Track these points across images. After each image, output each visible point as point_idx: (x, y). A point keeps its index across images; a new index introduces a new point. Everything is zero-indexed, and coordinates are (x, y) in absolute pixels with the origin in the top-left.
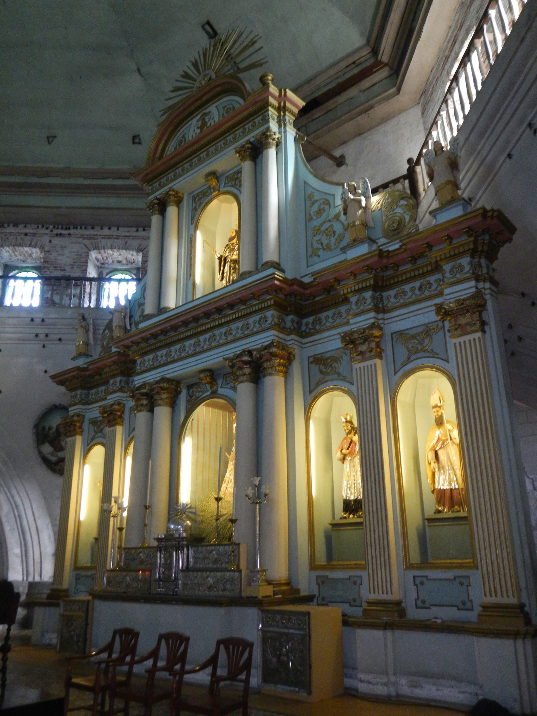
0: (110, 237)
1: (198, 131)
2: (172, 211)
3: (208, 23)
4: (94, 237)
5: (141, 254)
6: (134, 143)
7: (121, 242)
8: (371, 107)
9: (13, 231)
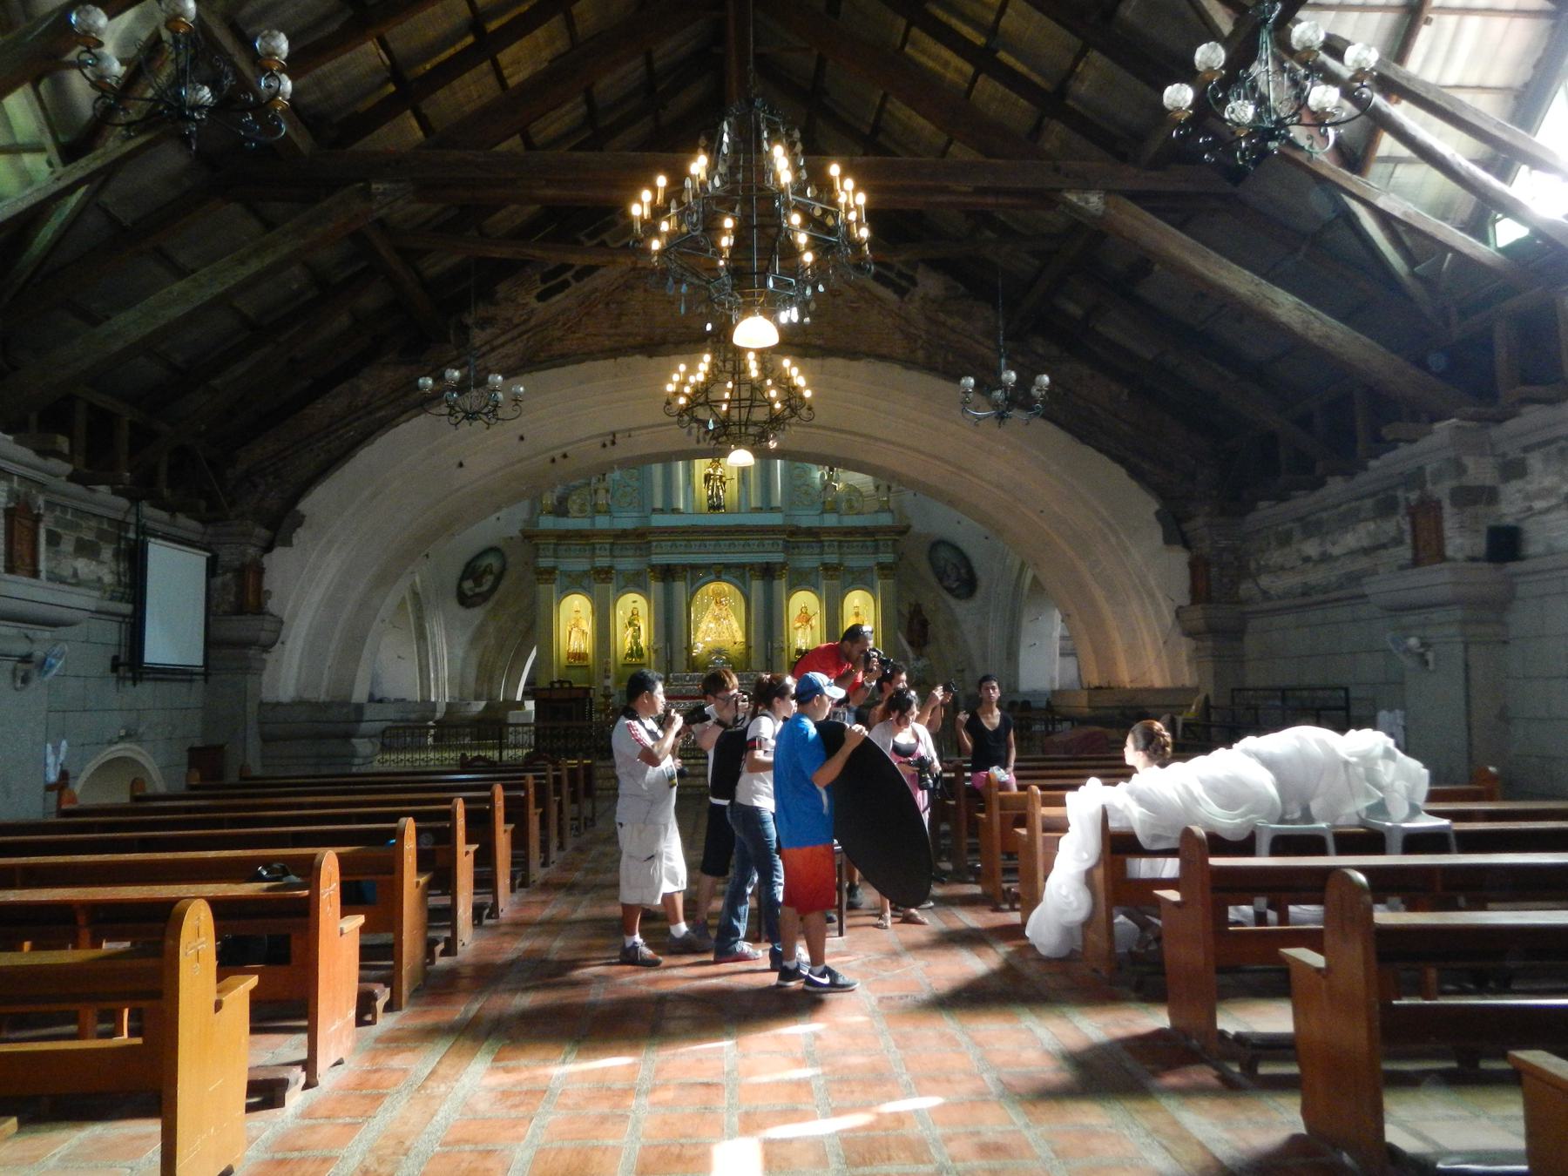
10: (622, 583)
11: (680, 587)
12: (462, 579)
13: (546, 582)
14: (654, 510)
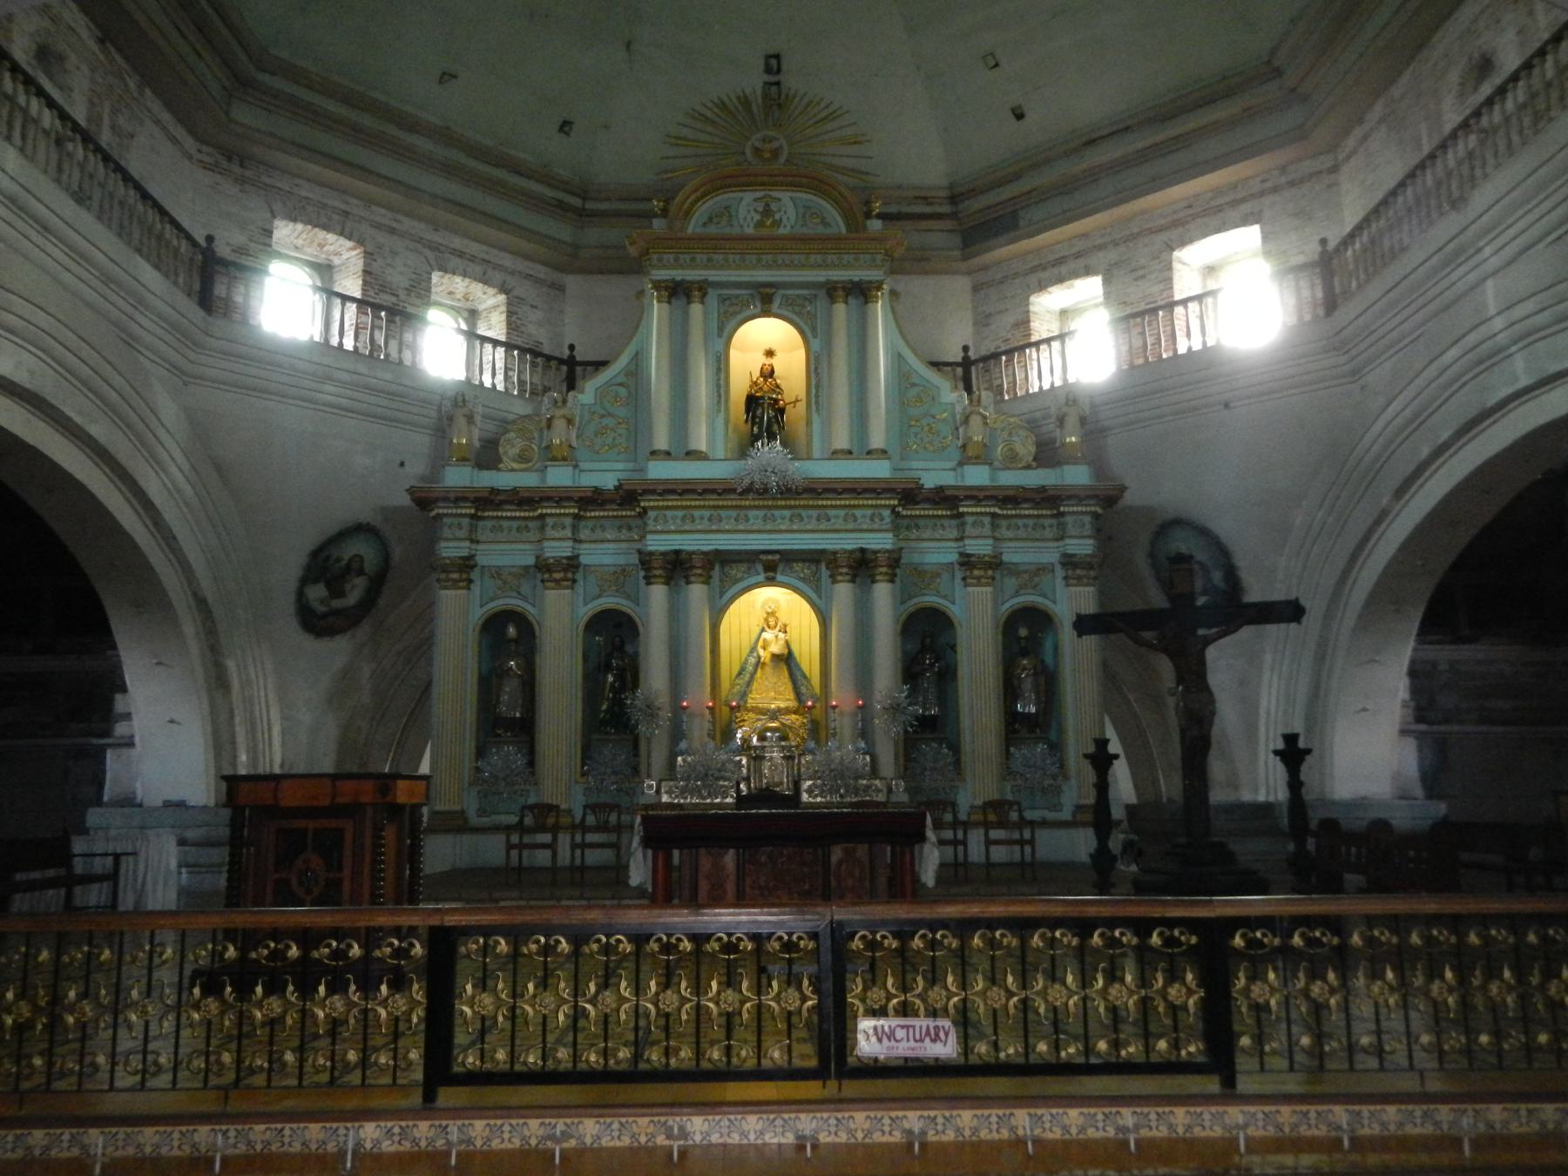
0: (460, 254)
1: (757, 217)
2: (696, 309)
3: (777, 57)
4: (435, 247)
5: (502, 298)
6: (561, 129)
7: (478, 269)
8: (928, 259)
9: (310, 195)
10: (596, 591)
11: (697, 592)
12: (305, 581)
13: (455, 585)
14: (653, 453)
